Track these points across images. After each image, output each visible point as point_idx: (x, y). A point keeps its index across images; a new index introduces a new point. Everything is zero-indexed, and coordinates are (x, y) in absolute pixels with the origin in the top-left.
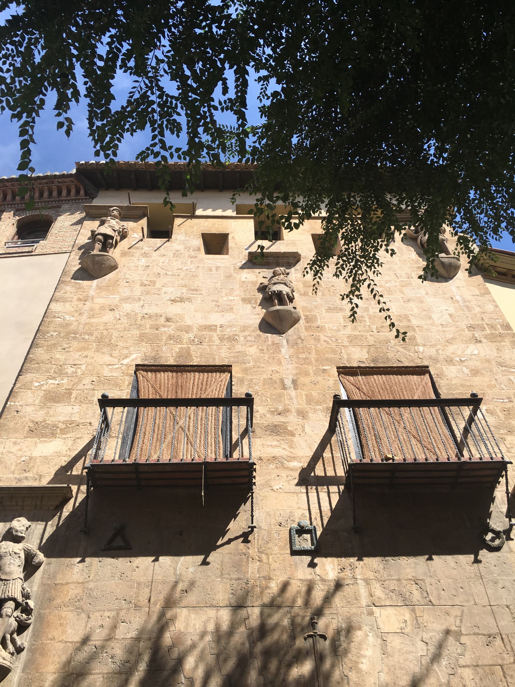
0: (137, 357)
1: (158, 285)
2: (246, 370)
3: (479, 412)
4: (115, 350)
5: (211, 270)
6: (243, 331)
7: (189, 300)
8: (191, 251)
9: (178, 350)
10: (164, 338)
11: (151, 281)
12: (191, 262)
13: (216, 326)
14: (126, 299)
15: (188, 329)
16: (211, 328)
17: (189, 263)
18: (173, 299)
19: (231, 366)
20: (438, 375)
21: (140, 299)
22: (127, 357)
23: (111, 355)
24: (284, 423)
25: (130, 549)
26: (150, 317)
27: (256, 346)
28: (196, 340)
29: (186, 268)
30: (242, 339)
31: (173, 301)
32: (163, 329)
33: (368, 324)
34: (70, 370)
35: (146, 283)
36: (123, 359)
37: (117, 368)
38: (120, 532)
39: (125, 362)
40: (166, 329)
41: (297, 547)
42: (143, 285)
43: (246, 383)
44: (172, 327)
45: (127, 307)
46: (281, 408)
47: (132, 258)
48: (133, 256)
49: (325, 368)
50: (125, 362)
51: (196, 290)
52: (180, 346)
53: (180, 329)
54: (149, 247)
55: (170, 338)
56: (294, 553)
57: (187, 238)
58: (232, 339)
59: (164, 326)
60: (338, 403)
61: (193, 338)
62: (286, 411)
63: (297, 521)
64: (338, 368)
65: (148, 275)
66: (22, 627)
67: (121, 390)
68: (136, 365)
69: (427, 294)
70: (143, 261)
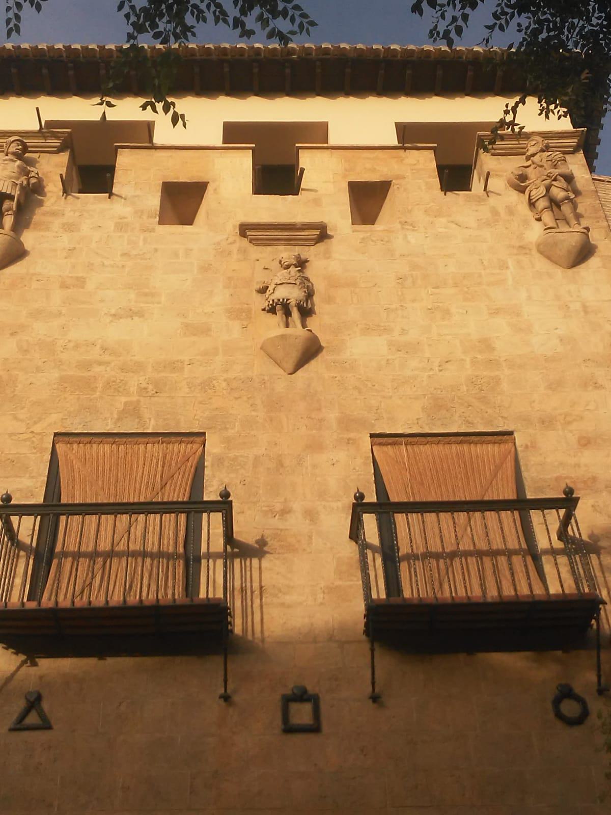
0: (55, 422)
1: (90, 286)
2: (228, 442)
3: (573, 521)
4: (23, 408)
5: (176, 255)
6: (226, 371)
7: (141, 314)
8: (145, 217)
9: (121, 407)
10: (100, 385)
11: (78, 278)
12: (145, 240)
13: (182, 362)
14: (37, 314)
15: (138, 367)
16: (174, 366)
17: (141, 243)
18: (113, 311)
19: (204, 434)
20: (527, 447)
21: (60, 314)
22: (40, 419)
23: (15, 418)
24: (281, 530)
25: (49, 727)
26: (77, 346)
27: (245, 398)
28: (150, 387)
29: (134, 252)
30: (224, 384)
31: (114, 315)
32: (97, 369)
33: (427, 355)
36: (35, 423)
37: (25, 440)
39: (37, 428)
40: (102, 368)
42: (64, 286)
43: (226, 464)
44: (113, 364)
45: (40, 329)
46: (278, 507)
47: (47, 234)
48: (48, 229)
49: (352, 435)
52: (124, 399)
54: (74, 211)
55: (108, 385)
57: (138, 193)
58: (207, 385)
59: (100, 363)
60: (359, 507)
61: (144, 385)
62: (285, 512)
63: (291, 685)
64: (372, 436)
65: (74, 267)
67: (32, 477)
68: (56, 434)
69: (529, 298)
70: (65, 240)
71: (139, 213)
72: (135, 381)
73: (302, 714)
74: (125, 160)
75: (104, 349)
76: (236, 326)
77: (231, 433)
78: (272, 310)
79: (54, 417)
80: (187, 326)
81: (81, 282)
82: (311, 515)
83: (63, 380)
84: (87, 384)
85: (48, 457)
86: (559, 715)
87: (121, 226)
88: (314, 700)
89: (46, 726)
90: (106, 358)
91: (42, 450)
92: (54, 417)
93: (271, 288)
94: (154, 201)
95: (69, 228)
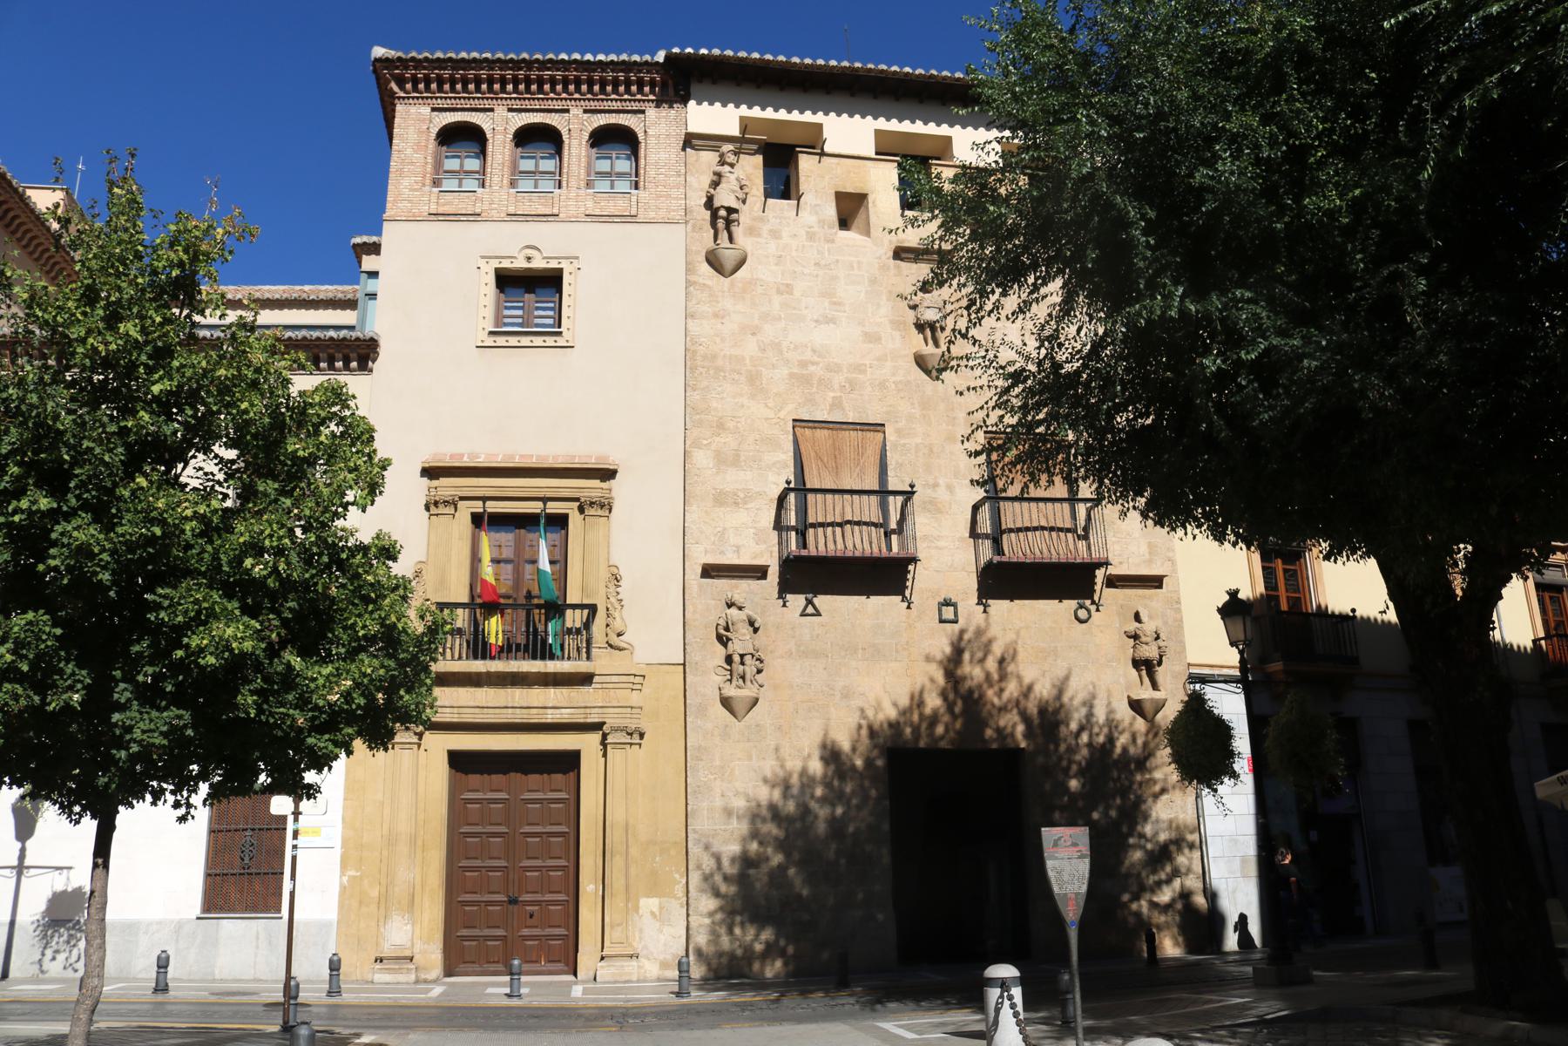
1: (797, 293)
2: (898, 432)
11: (787, 285)
15: (834, 368)
16: (860, 369)
26: (796, 348)
32: (812, 368)
34: (731, 425)
35: (782, 288)
38: (809, 602)
39: (782, 415)
41: (945, 617)
42: (779, 292)
45: (770, 332)
46: (931, 482)
50: (782, 415)
51: (840, 304)
53: (829, 369)
55: (820, 380)
56: (942, 621)
58: (882, 385)
62: (936, 485)
66: (759, 671)
70: (772, 248)
71: (821, 222)
72: (838, 379)
73: (948, 613)
74: (806, 163)
75: (814, 351)
76: (897, 334)
77: (900, 425)
78: (920, 327)
79: (790, 407)
80: (866, 334)
81: (789, 289)
82: (950, 488)
83: (792, 375)
84: (805, 380)
85: (791, 437)
86: (1077, 618)
87: (811, 236)
88: (955, 605)
89: (818, 614)
90: (816, 359)
91: (787, 433)
92: (790, 407)
93: (920, 309)
94: (831, 212)
95: (775, 234)
